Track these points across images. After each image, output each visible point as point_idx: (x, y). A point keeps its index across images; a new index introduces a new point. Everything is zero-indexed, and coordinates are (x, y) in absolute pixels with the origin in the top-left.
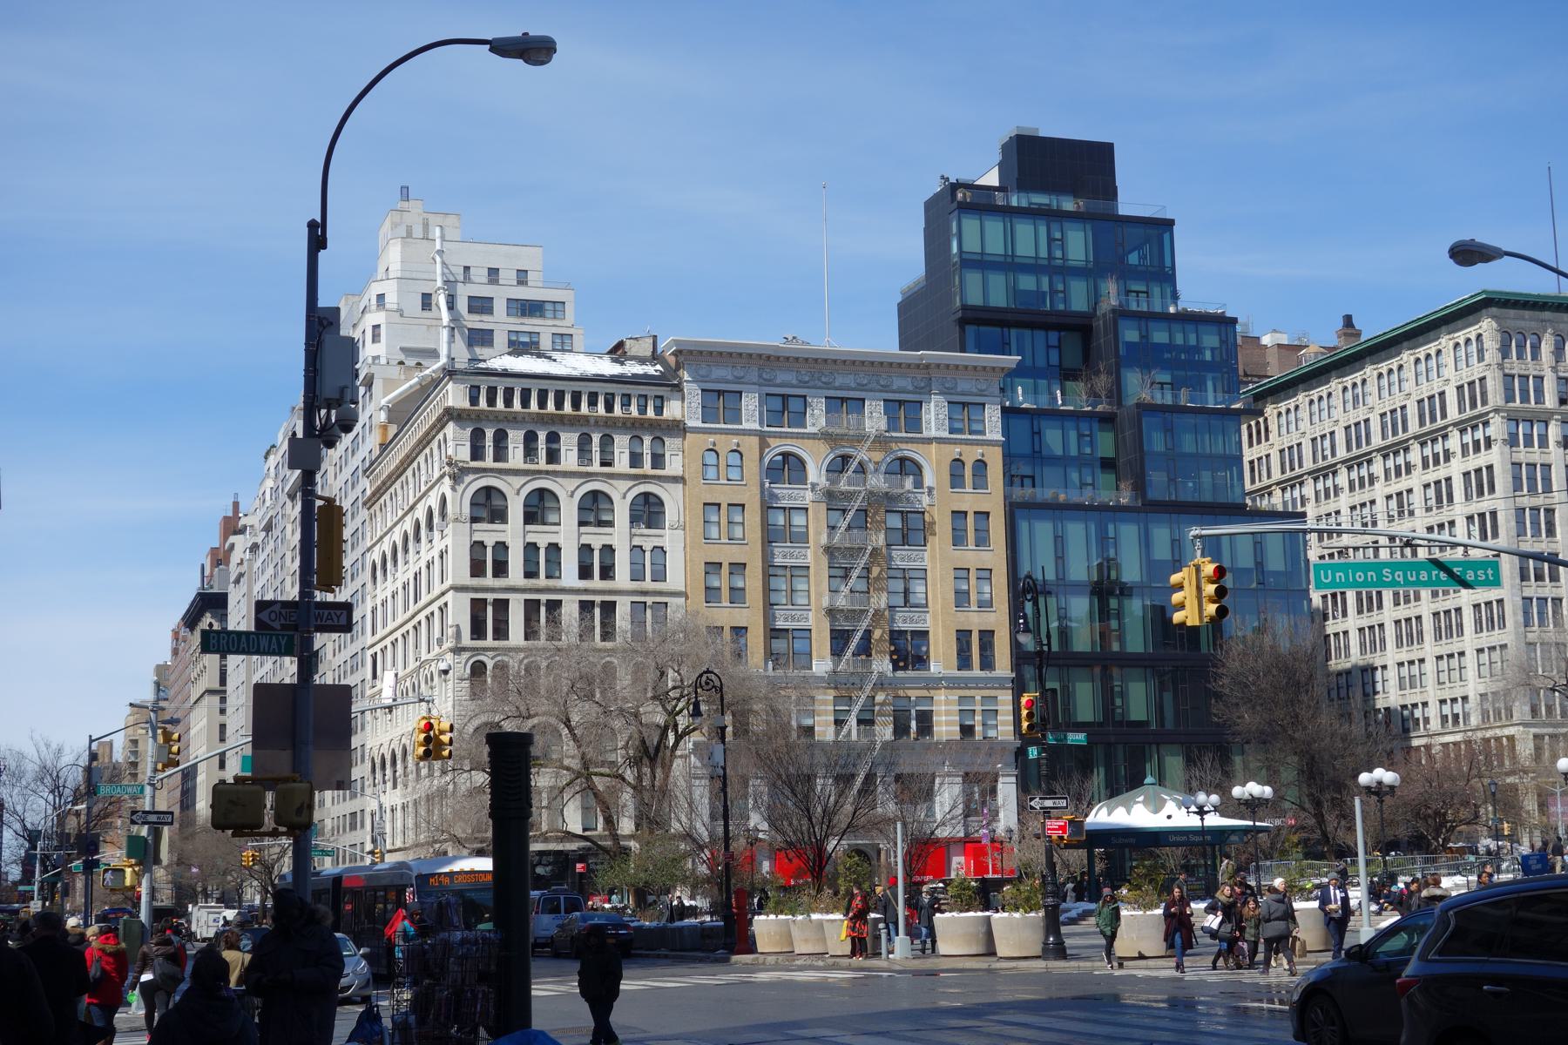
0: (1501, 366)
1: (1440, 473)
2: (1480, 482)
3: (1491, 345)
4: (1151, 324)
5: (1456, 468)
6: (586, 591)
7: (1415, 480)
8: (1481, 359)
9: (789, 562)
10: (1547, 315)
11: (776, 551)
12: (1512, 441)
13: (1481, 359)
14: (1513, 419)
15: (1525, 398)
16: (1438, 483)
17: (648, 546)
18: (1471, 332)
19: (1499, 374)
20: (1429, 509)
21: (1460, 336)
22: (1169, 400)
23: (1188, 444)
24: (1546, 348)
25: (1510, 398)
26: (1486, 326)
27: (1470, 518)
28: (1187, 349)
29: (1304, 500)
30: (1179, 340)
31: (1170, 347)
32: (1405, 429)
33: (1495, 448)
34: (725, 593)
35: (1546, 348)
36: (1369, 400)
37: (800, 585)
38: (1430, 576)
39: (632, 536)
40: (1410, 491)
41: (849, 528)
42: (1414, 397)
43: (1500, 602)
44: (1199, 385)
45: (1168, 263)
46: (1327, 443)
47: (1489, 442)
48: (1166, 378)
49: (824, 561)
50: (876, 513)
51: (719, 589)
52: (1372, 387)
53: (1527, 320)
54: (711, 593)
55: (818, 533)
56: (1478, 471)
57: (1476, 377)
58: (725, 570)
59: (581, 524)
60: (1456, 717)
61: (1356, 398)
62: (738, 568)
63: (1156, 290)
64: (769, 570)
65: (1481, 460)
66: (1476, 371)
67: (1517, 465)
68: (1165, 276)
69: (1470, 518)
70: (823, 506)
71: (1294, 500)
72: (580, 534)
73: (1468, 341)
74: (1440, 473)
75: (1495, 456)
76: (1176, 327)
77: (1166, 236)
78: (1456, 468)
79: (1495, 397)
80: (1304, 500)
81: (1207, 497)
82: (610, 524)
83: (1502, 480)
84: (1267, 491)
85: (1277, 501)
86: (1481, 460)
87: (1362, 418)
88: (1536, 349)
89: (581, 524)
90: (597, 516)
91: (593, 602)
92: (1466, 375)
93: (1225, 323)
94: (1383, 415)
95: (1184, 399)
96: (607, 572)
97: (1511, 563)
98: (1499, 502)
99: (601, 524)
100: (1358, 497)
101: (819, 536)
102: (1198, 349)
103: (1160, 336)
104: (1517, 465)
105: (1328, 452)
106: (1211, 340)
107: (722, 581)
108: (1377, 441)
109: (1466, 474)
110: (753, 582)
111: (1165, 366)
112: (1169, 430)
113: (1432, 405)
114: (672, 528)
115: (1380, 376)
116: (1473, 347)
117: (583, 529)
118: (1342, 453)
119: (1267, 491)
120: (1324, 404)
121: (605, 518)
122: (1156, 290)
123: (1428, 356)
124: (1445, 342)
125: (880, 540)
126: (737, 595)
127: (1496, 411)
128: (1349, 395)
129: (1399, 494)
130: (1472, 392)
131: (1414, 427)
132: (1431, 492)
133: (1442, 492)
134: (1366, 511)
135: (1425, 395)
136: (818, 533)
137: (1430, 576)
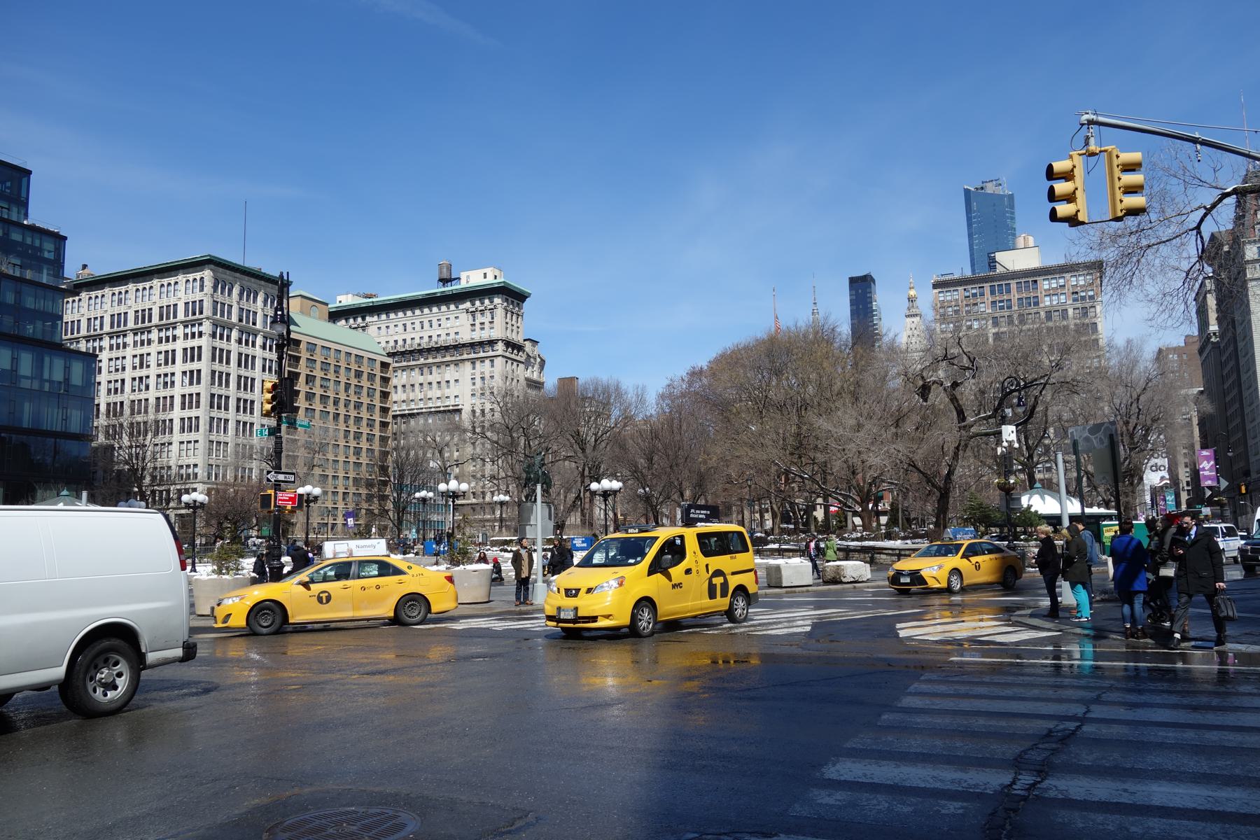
0: (212, 296)
1: (170, 346)
2: (193, 354)
3: (208, 284)
4: (12, 228)
5: (179, 346)
7: (153, 349)
8: (202, 289)
10: (238, 275)
12: (214, 335)
13: (202, 289)
14: (215, 325)
15: (222, 315)
16: (167, 352)
18: (198, 275)
19: (211, 300)
20: (159, 365)
21: (191, 277)
22: (18, 274)
23: (30, 303)
24: (236, 291)
25: (215, 313)
26: (207, 274)
27: (184, 373)
28: (32, 247)
29: (101, 349)
30: (29, 241)
31: (22, 244)
32: (150, 321)
33: (204, 338)
35: (236, 291)
36: (129, 302)
40: (149, 354)
42: (158, 305)
43: (197, 418)
44: (40, 271)
45: (24, 194)
46: (98, 322)
47: (200, 334)
48: (18, 262)
52: (131, 295)
53: (227, 276)
56: (192, 349)
57: (197, 299)
60: (188, 475)
61: (120, 301)
63: (15, 209)
65: (196, 343)
66: (198, 296)
67: (214, 349)
68: (24, 204)
69: (184, 373)
71: (94, 348)
73: (195, 280)
74: (170, 346)
75: (205, 342)
76: (28, 233)
77: (25, 180)
78: (179, 346)
79: (207, 311)
80: (101, 349)
81: (39, 336)
83: (206, 354)
84: (77, 340)
85: (83, 346)
86: (196, 343)
87: (122, 311)
88: (230, 291)
92: (191, 298)
93: (60, 240)
94: (137, 312)
95: (29, 275)
98: (204, 365)
100: (114, 354)
102: (41, 249)
103: (16, 236)
104: (214, 349)
105: (98, 327)
106: (49, 246)
108: (131, 325)
109: (185, 350)
111: (19, 255)
112: (18, 293)
113: (168, 311)
115: (137, 290)
116: (198, 284)
118: (107, 328)
119: (77, 340)
120: (99, 301)
122: (15, 209)
123: (169, 284)
124: (181, 278)
127: (208, 318)
128: (116, 298)
129: (142, 355)
130: (194, 308)
131: (155, 320)
132: (162, 357)
133: (169, 358)
134: (119, 362)
135: (165, 304)
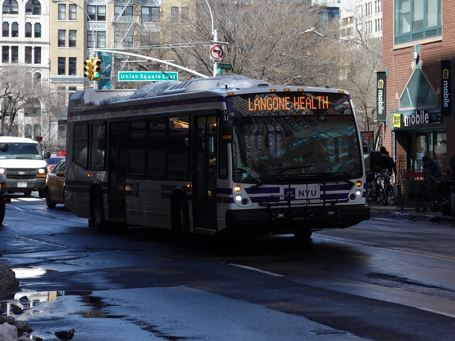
6: (5, 42)
9: (97, 29)
11: (90, 24)
17: (33, 23)
34: (67, 43)
37: (102, 40)
38: (155, 77)
39: (26, 18)
41: (124, 14)
49: (112, 28)
50: (136, 7)
51: (64, 41)
54: (61, 43)
55: (110, 17)
58: (67, 33)
59: (4, 13)
62: (73, 32)
64: (88, 34)
70: (113, 5)
72: (3, 18)
82: (16, 13)
89: (4, 13)
90: (11, 9)
91: (8, 47)
96: (15, 34)
97: (81, 89)
99: (12, 12)
101: (110, 18)
107: (66, 38)
110: (80, 39)
114: (44, 15)
117: (4, 15)
121: (14, 10)
125: (137, 20)
126: (72, 44)
136: (110, 17)
137: (155, 77)
